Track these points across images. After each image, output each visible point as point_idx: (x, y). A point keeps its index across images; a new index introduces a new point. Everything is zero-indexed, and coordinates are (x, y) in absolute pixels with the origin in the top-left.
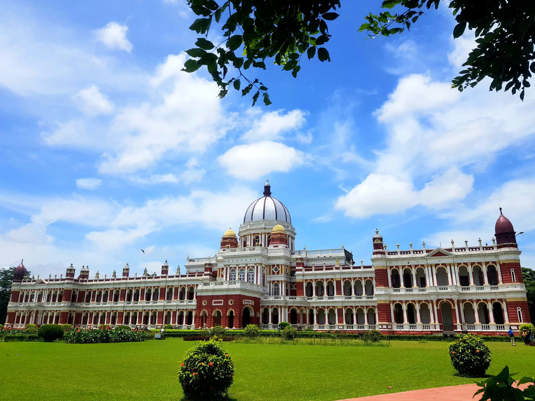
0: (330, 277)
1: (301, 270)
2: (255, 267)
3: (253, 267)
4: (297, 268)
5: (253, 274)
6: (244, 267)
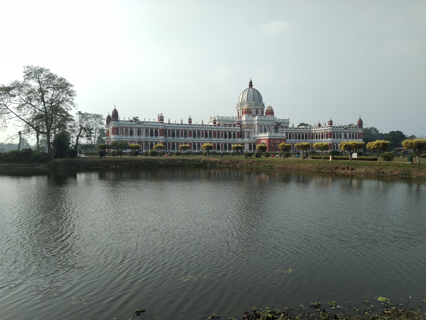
0: (290, 131)
1: (280, 128)
2: (271, 126)
3: (270, 126)
4: (279, 127)
5: (269, 129)
6: (266, 125)
